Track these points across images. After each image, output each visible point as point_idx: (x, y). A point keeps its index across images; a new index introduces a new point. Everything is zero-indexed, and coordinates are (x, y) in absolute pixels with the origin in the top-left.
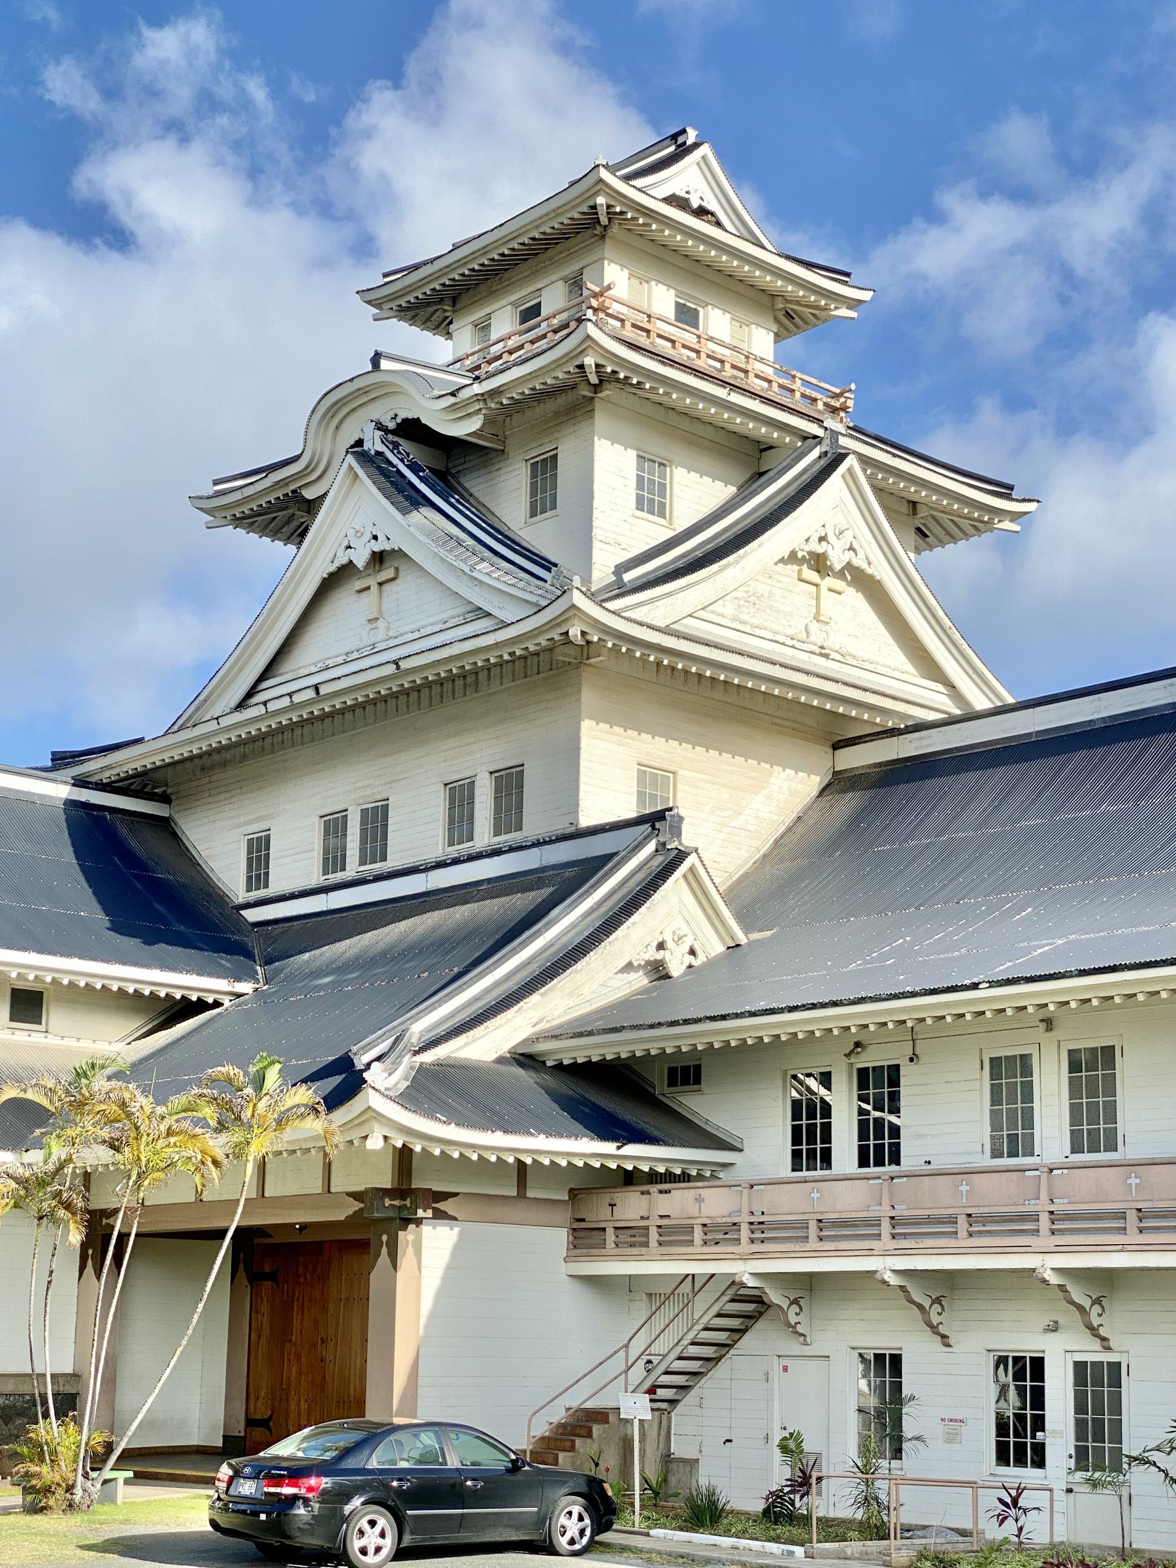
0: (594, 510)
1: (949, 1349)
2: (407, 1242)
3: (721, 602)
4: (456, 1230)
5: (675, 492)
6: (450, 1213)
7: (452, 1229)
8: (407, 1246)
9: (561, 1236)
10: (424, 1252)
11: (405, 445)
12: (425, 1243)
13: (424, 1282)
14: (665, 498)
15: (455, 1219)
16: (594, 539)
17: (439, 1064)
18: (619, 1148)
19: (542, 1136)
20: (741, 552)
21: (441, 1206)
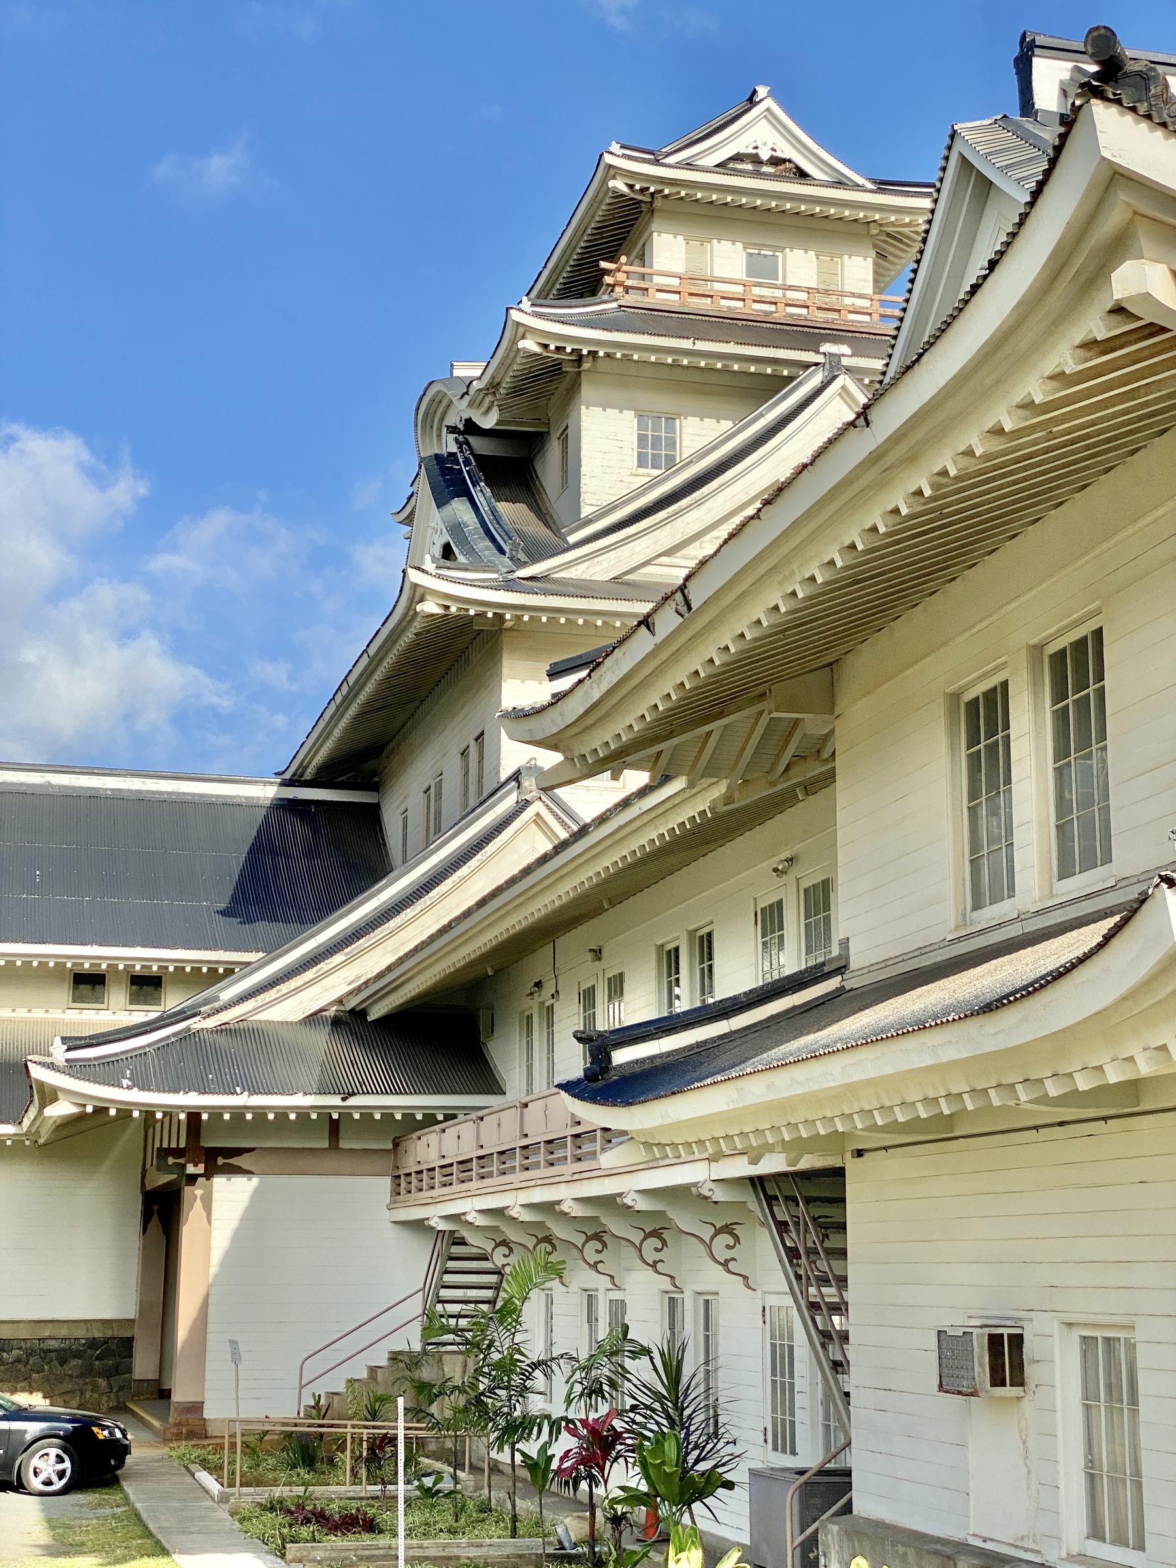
0: (582, 477)
1: (564, 1289)
2: (196, 1197)
3: (697, 544)
4: (255, 1181)
5: (684, 444)
6: (244, 1168)
7: (250, 1179)
8: (195, 1201)
9: (385, 1184)
10: (215, 1206)
11: (471, 439)
12: (215, 1196)
13: (215, 1233)
14: (675, 451)
15: (252, 1173)
16: (582, 504)
17: (223, 1029)
18: (344, 1099)
19: (246, 1093)
20: (697, 494)
21: (235, 1161)
